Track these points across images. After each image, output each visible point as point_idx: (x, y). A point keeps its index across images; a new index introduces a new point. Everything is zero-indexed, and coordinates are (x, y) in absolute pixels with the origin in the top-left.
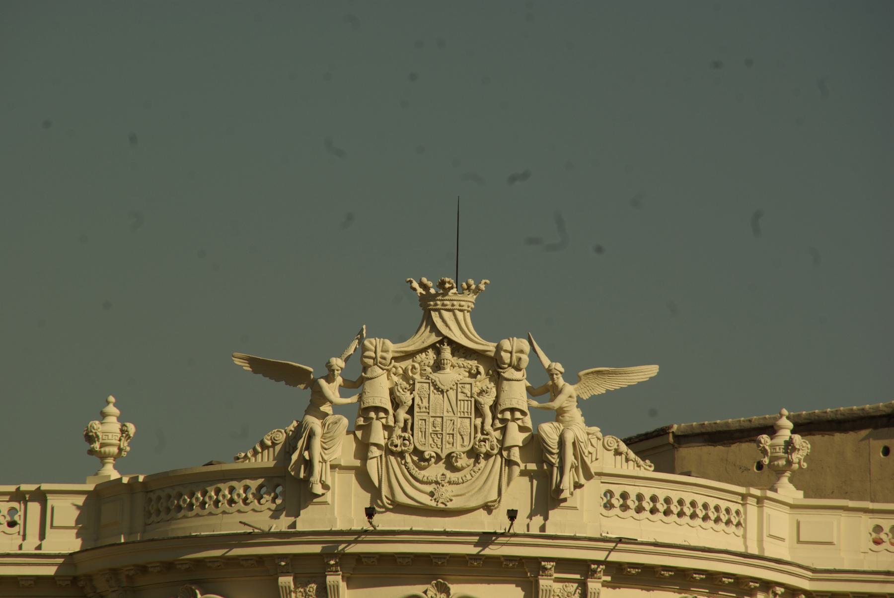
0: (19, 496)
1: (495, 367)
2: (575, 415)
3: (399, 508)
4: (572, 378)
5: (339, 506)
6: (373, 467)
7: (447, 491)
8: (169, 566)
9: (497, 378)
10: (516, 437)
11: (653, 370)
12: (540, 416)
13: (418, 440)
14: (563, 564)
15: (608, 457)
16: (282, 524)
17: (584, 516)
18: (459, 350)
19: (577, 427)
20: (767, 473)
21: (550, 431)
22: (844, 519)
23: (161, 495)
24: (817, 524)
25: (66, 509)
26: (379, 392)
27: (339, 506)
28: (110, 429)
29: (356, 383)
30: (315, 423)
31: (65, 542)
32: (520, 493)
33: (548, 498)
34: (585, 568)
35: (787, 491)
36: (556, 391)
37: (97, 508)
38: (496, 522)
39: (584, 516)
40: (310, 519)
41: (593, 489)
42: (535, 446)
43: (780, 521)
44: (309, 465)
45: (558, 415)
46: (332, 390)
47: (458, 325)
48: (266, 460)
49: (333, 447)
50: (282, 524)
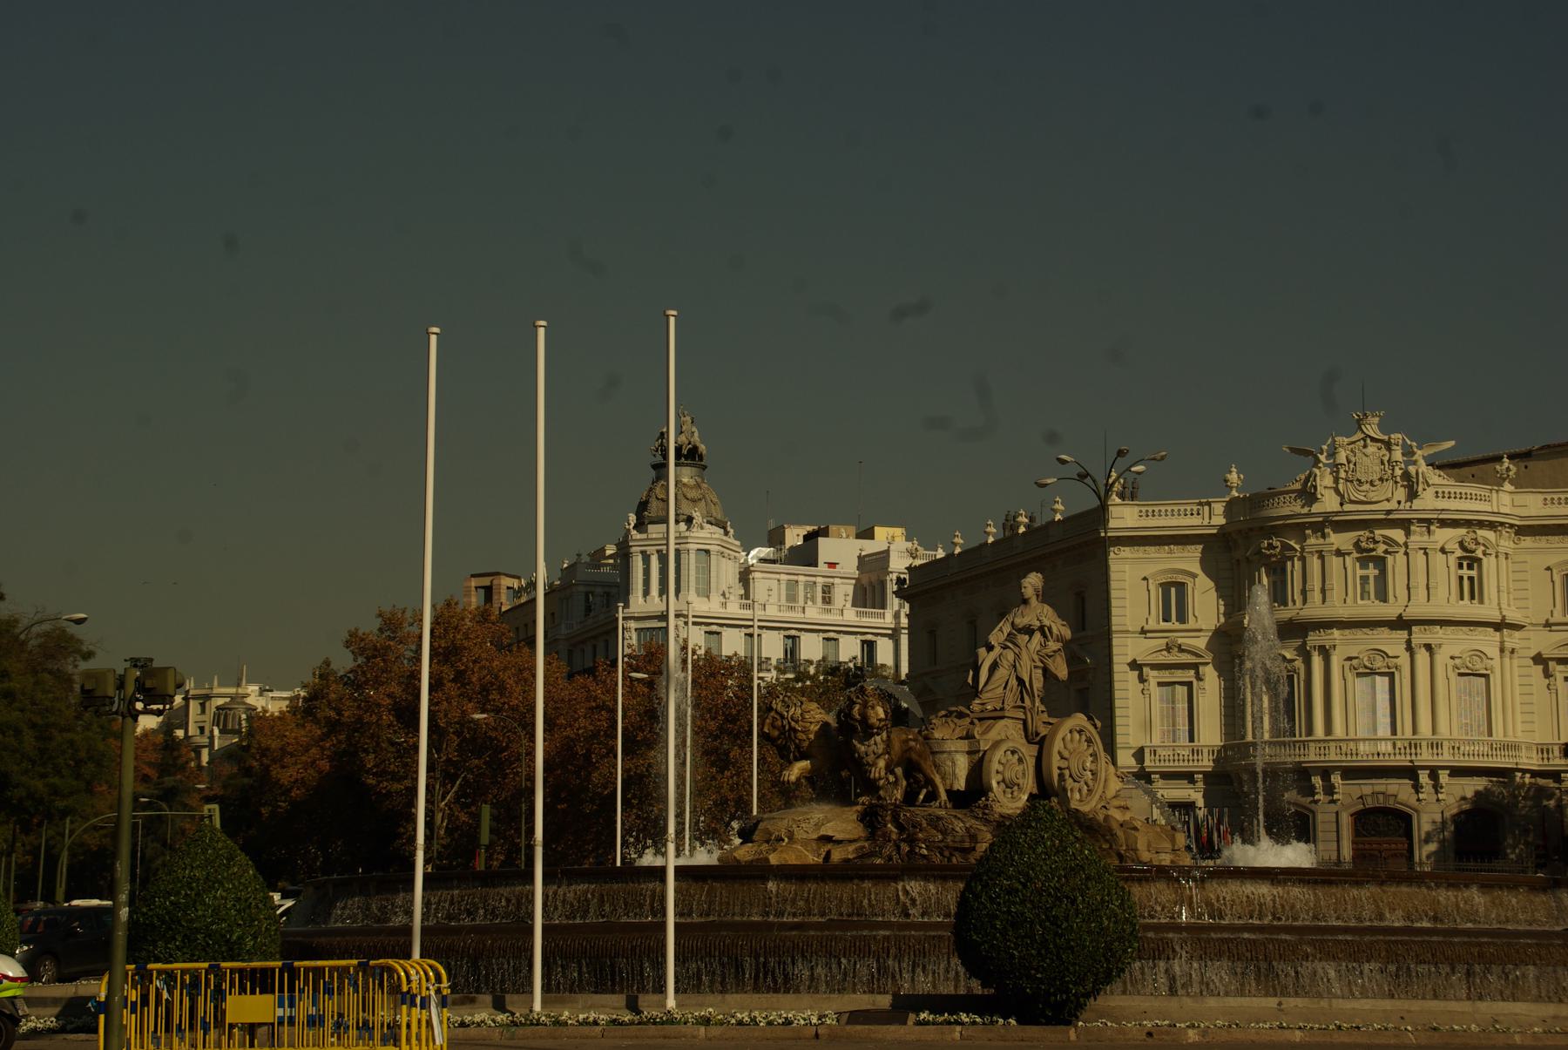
0: (1200, 504)
1: (1388, 445)
2: (1422, 462)
3: (1352, 502)
4: (1420, 448)
5: (1328, 502)
6: (1341, 487)
7: (1371, 495)
8: (1262, 528)
9: (1389, 450)
10: (1398, 472)
11: (1453, 443)
12: (1407, 463)
13: (1358, 475)
14: (1420, 520)
15: (1435, 477)
16: (1306, 510)
17: (1427, 501)
18: (1373, 440)
19: (1423, 467)
20: (1499, 481)
21: (1412, 469)
22: (1531, 496)
23: (1255, 502)
24: (1519, 499)
25: (1219, 508)
26: (1342, 457)
27: (1328, 502)
28: (1233, 477)
29: (1332, 454)
30: (1316, 471)
31: (1220, 520)
32: (1401, 493)
33: (1412, 495)
34: (1429, 522)
35: (1508, 486)
36: (1414, 453)
37: (1231, 507)
38: (1393, 505)
39: (1427, 501)
40: (1316, 508)
41: (1431, 491)
42: (1406, 475)
43: (1505, 499)
44: (1315, 488)
45: (1415, 463)
46: (1322, 458)
47: (1372, 429)
48: (1298, 486)
49: (1324, 480)
50: (1306, 510)
